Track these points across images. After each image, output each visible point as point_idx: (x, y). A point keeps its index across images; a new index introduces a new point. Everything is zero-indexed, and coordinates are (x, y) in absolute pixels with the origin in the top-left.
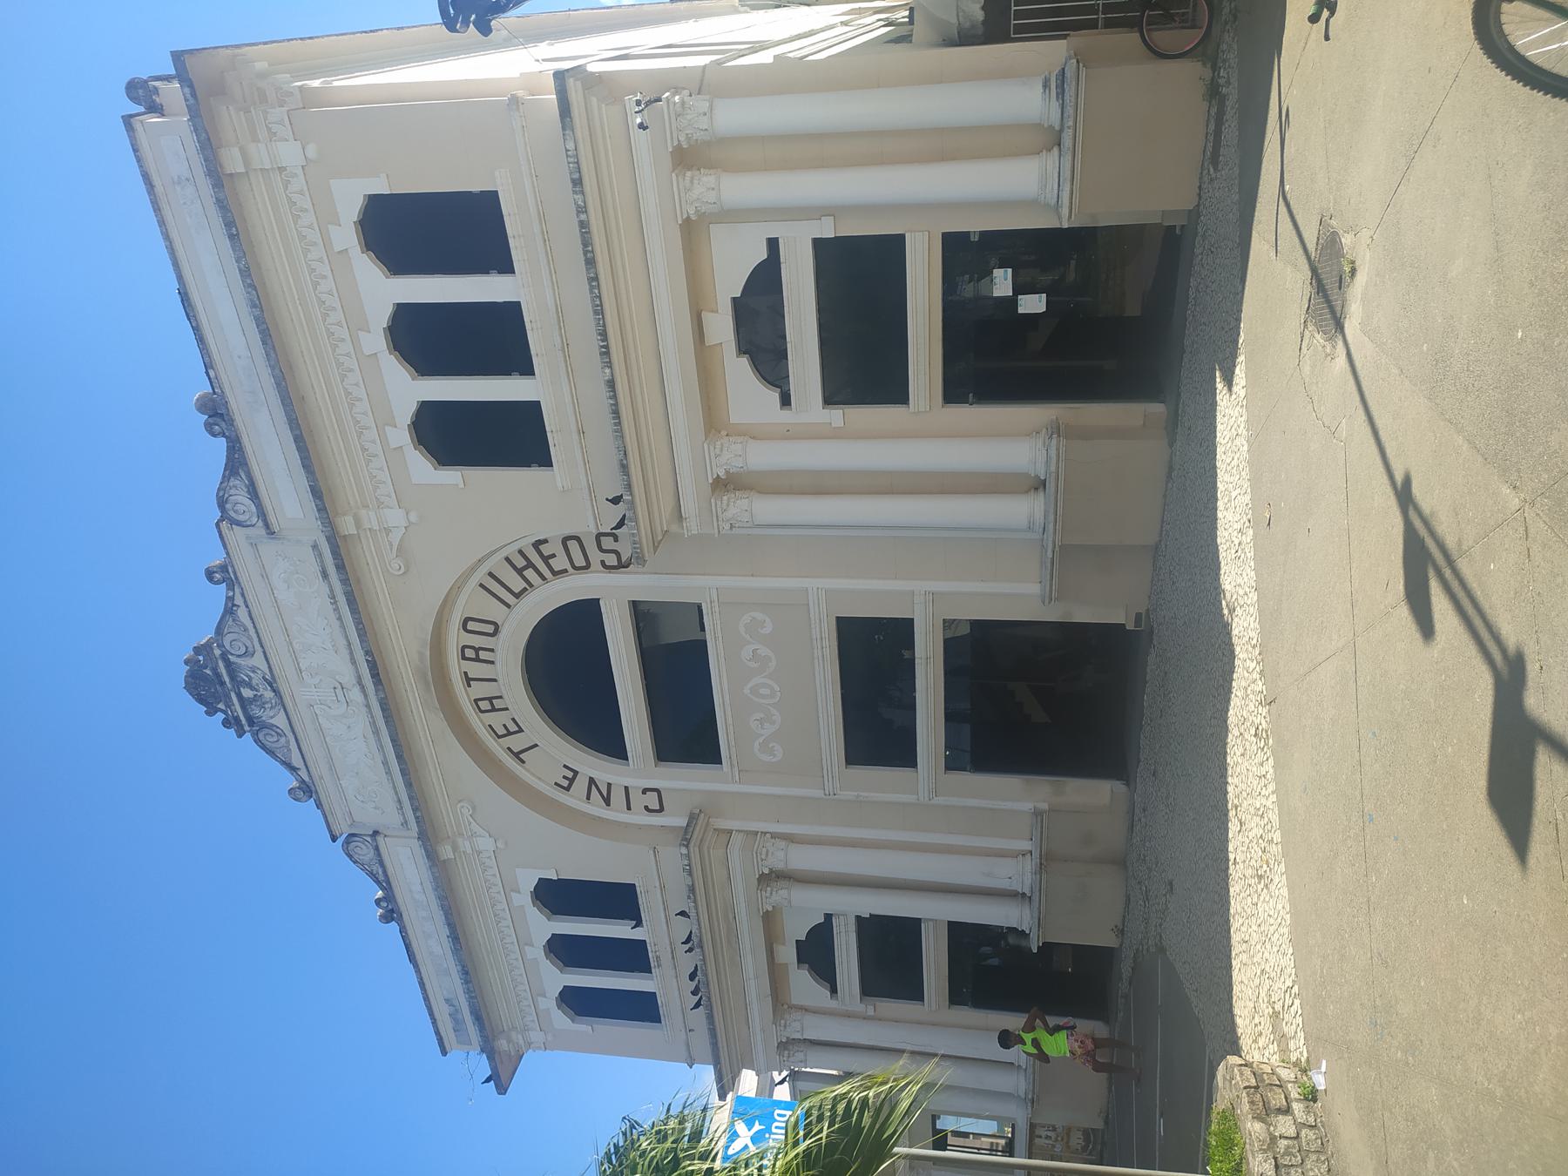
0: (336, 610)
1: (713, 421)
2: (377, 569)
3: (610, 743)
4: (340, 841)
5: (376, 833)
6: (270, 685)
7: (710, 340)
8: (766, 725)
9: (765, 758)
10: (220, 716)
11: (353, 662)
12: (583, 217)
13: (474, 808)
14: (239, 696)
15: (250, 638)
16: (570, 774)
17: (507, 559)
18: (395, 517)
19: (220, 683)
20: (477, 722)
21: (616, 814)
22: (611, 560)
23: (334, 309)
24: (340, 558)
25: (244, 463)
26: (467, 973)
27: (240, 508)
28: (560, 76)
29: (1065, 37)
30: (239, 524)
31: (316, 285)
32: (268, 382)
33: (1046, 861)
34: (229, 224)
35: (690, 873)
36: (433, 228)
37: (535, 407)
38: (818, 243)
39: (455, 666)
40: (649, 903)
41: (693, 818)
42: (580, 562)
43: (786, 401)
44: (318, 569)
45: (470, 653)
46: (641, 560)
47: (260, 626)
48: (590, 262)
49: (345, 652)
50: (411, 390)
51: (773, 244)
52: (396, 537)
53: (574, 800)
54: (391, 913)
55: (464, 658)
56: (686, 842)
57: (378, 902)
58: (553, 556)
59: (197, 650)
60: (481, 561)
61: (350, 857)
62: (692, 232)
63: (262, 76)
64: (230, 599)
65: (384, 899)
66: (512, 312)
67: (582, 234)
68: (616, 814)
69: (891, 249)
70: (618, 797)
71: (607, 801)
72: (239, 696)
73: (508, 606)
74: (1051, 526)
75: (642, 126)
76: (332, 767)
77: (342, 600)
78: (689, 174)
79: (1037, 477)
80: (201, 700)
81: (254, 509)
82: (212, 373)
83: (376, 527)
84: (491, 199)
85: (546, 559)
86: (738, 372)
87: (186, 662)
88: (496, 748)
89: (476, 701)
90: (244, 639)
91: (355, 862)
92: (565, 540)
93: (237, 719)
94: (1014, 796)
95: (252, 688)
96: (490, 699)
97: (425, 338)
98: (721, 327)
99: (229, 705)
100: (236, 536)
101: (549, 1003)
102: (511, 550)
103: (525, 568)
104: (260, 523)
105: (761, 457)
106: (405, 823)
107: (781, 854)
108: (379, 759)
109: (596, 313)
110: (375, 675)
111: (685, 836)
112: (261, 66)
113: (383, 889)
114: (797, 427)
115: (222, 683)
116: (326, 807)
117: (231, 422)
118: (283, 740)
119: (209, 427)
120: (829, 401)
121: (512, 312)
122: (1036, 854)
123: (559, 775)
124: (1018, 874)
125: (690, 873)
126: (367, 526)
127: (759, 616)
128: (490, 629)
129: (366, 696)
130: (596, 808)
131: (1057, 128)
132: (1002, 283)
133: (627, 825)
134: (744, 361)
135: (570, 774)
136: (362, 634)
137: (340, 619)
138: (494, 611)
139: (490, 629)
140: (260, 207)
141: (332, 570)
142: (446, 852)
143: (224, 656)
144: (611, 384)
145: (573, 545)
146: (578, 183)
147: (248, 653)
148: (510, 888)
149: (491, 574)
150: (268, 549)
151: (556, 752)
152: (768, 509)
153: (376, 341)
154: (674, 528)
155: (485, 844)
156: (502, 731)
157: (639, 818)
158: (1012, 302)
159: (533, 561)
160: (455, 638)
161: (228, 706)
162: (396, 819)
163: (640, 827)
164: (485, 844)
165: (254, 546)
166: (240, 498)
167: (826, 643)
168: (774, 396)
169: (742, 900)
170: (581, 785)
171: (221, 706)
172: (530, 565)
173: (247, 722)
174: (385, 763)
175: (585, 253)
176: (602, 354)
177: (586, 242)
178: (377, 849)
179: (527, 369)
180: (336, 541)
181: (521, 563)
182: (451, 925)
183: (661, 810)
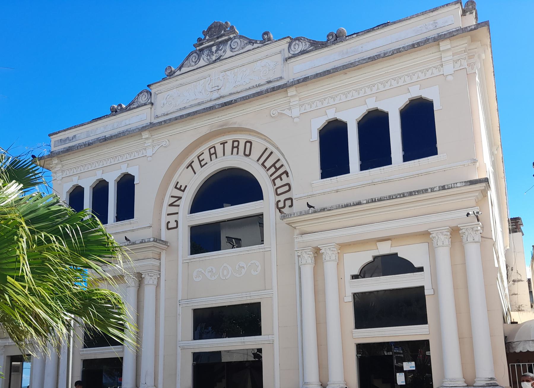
0: (253, 87)
1: (344, 247)
4: (148, 89)
5: (152, 104)
6: (218, 59)
10: (203, 37)
11: (231, 94)
12: (429, 190)
13: (165, 147)
14: (213, 45)
15: (239, 50)
16: (182, 188)
17: (279, 160)
18: (296, 112)
20: (204, 148)
22: (281, 205)
26: (89, 145)
27: (297, 47)
28: (486, 180)
29: (511, 386)
31: (394, 79)
32: (352, 59)
34: (419, 44)
35: (141, 242)
36: (420, 128)
37: (347, 171)
38: (422, 288)
39: (229, 138)
40: (126, 225)
41: (165, 243)
42: (279, 191)
43: (355, 277)
44: (271, 79)
45: (236, 144)
47: (245, 54)
48: (411, 194)
49: (235, 90)
50: (352, 120)
51: (421, 269)
52: (287, 112)
53: (171, 191)
54: (115, 112)
55: (234, 142)
58: (281, 180)
59: (232, 27)
60: (277, 148)
61: (141, 93)
62: (426, 235)
63: (479, 57)
65: (122, 108)
66: (388, 161)
67: (423, 190)
69: (422, 319)
70: (173, 210)
72: (213, 45)
73: (258, 160)
75: (468, 214)
76: (181, 85)
77: (258, 90)
78: (449, 234)
80: (210, 29)
82: (355, 35)
84: (433, 151)
85: (280, 176)
86: (366, 257)
87: (226, 23)
88: (193, 156)
89: (214, 147)
90: (238, 48)
92: (288, 184)
93: (202, 44)
95: (216, 51)
96: (215, 153)
97: (374, 125)
98: (385, 249)
100: (284, 44)
101: (76, 181)
102: (283, 161)
103: (275, 168)
104: (290, 55)
105: (330, 268)
106: (157, 117)
107: (151, 282)
108: (187, 105)
109: (390, 196)
112: (483, 56)
113: (126, 108)
115: (218, 38)
117: (334, 43)
118: (193, 64)
119: (331, 34)
121: (388, 161)
123: (182, 183)
125: (141, 242)
128: (247, 152)
129: (215, 100)
130: (168, 200)
131: (474, 385)
132: (409, 366)
133: (160, 214)
134: (371, 259)
135: (182, 188)
137: (250, 88)
138: (255, 155)
139: (247, 152)
140: (426, 56)
141: (271, 85)
142: (145, 135)
143: (230, 39)
144: (359, 203)
145: (287, 188)
146: (443, 188)
147: (232, 49)
149: (272, 153)
150: (279, 58)
151: (194, 182)
152: (308, 272)
154: (297, 232)
155: (149, 152)
156: (201, 158)
158: (401, 370)
159: (279, 171)
160: (242, 138)
161: (208, 40)
162: (159, 112)
163: (160, 220)
164: (149, 152)
165: (280, 52)
167: (249, 298)
168: (357, 272)
170: (178, 193)
171: (207, 37)
172: (277, 170)
174: (185, 108)
175: (414, 192)
176: (372, 199)
177: (419, 192)
178: (145, 104)
180: (285, 87)
181: (278, 165)
182: (111, 138)
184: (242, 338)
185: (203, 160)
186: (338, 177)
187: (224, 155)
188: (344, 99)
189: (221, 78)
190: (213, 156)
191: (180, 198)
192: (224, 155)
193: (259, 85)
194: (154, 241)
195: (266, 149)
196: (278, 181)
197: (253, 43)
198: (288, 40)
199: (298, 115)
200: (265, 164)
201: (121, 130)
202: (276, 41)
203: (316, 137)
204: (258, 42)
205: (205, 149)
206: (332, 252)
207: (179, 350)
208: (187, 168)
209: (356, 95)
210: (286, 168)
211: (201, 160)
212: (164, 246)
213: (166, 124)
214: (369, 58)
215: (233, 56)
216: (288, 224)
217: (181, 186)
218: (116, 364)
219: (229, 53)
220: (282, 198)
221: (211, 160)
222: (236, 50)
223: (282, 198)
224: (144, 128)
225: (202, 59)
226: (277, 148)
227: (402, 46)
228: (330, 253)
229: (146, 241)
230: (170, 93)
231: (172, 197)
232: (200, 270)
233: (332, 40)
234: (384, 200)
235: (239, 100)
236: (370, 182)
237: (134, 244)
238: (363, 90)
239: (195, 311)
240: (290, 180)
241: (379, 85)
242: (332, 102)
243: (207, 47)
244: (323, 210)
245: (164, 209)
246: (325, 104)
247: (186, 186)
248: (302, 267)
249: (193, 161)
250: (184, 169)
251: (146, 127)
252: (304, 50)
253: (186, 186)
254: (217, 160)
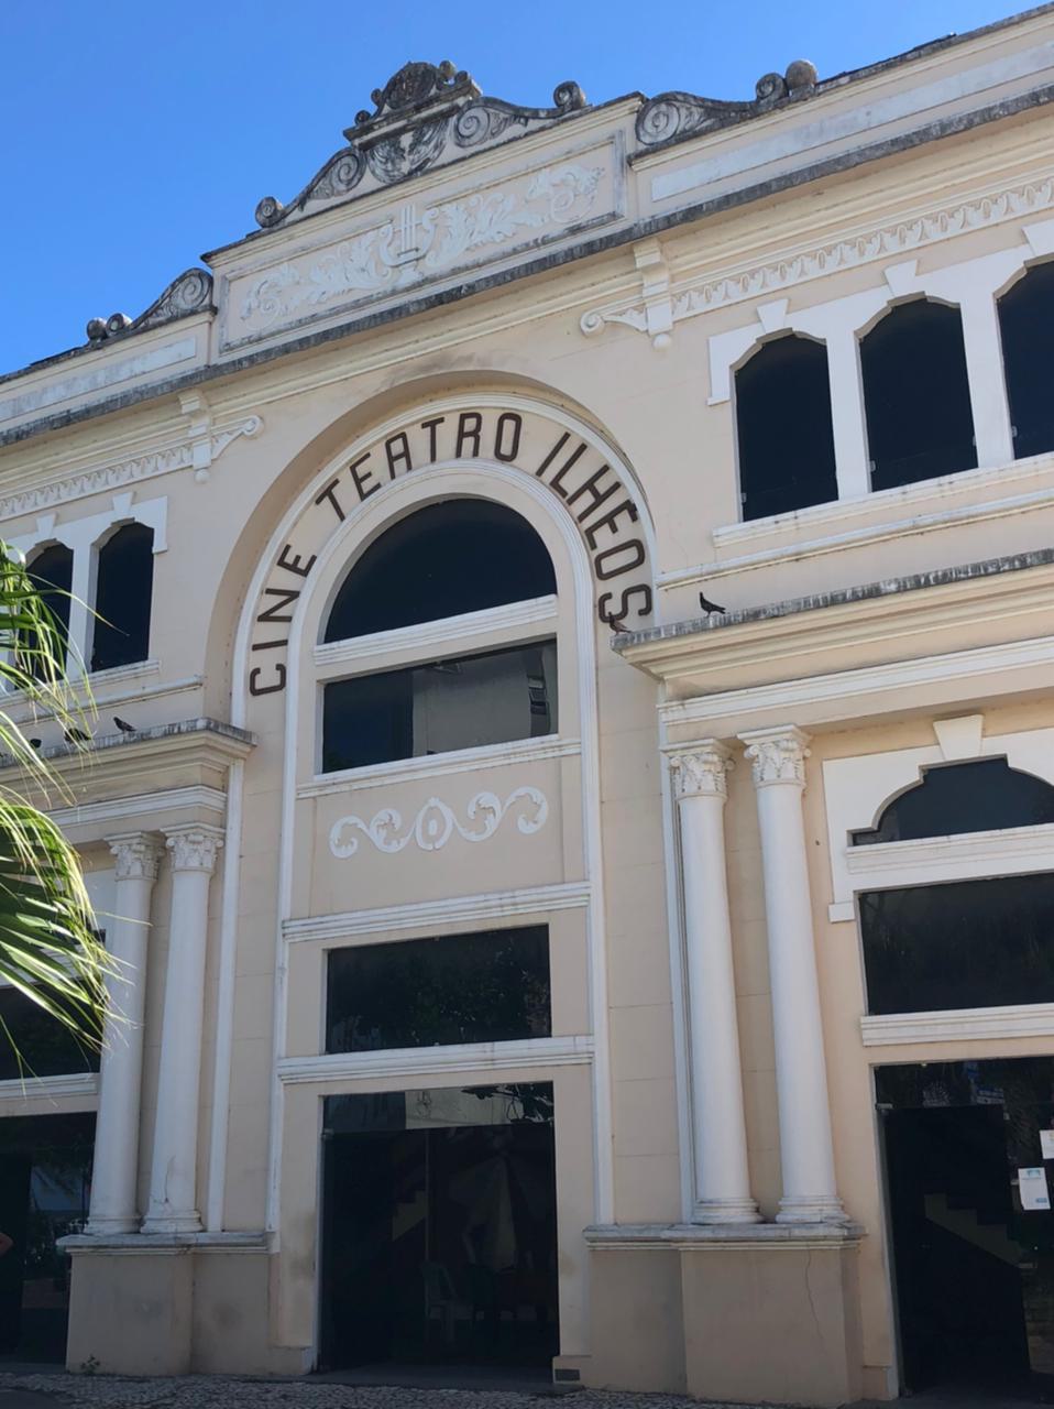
0: (527, 247)
2: (595, 293)
3: (346, 620)
4: (203, 266)
5: (214, 310)
6: (419, 168)
7: (944, 729)
8: (383, 833)
9: (335, 834)
10: (372, 109)
11: (455, 271)
13: (253, 437)
14: (403, 130)
16: (302, 565)
17: (605, 469)
18: (660, 317)
19: (417, 107)
21: (248, 630)
22: (613, 607)
23: (945, 229)
24: (603, 246)
25: (724, 123)
27: (662, 121)
30: (640, 121)
31: (976, 205)
32: (838, 150)
33: (193, 1253)
35: (168, 734)
37: (829, 493)
39: (449, 406)
40: (124, 681)
41: (244, 736)
42: (609, 565)
43: (858, 838)
44: (582, 221)
45: (470, 424)
46: (621, 645)
47: (499, 153)
49: (469, 259)
50: (841, 331)
52: (633, 319)
53: (267, 572)
54: (99, 337)
55: (463, 417)
56: (213, 727)
57: (117, 318)
58: (614, 529)
59: (462, 77)
60: (602, 433)
61: (181, 279)
64: (535, 114)
65: (122, 326)
68: (248, 630)
70: (271, 631)
71: (265, 617)
72: (403, 130)
73: (540, 472)
74: (707, 1233)
79: (779, 1209)
80: (394, 84)
81: (662, 138)
83: (645, 293)
85: (609, 519)
86: (899, 770)
87: (445, 65)
88: (337, 466)
89: (403, 436)
90: (481, 133)
91: (173, 286)
92: (637, 544)
93: (370, 129)
94: (290, 1199)
95: (413, 147)
96: (406, 454)
98: (962, 743)
99: (388, 119)
100: (623, 118)
102: (619, 471)
103: (595, 493)
104: (642, 147)
105: (779, 807)
106: (229, 347)
107: (194, 862)
109: (976, 568)
110: (439, 300)
111: (219, 726)
113: (136, 323)
114: (826, 858)
115: (418, 109)
116: (250, 245)
118: (342, 187)
120: (864, 899)
122: (203, 1238)
123: (301, 550)
124: (172, 1210)
125: (168, 734)
126: (646, 282)
127: (544, 814)
128: (506, 449)
129: (408, 290)
130: (255, 602)
134: (913, 777)
135: (302, 565)
136: (498, 280)
137: (515, 251)
138: (531, 455)
139: (506, 449)
142: (191, 401)
143: (456, 110)
144: (874, 593)
145: (630, 555)
147: (461, 139)
148: (136, 488)
149: (583, 448)
150: (607, 158)
151: (335, 544)
153: (905, 283)
154: (669, 689)
155: (202, 455)
156: (361, 471)
157: (242, 662)
159: (606, 503)
161: (387, 117)
162: (234, 336)
163: (229, 664)
164: (202, 455)
165: (611, 140)
166: (676, 121)
167: (509, 911)
168: (867, 821)
169: (126, 810)
170: (288, 580)
172: (600, 499)
173: (363, 143)
174: (314, 318)
176: (917, 578)
178: (193, 313)
179: (880, 481)
180: (628, 239)
182: (87, 414)
183: (255, 692)
184: (488, 1045)
185: (369, 475)
186: (800, 512)
187: (433, 458)
188: (813, 270)
189: (427, 224)
190: (401, 464)
191: (293, 595)
192: (433, 458)
193: (545, 241)
194: (207, 728)
195: (567, 436)
197: (527, 119)
198: (636, 103)
199: (668, 325)
201: (117, 390)
202: (598, 108)
203: (723, 389)
204: (542, 115)
205: (374, 444)
206: (783, 755)
207: (279, 1090)
208: (318, 501)
209: (853, 258)
210: (631, 491)
211: (360, 476)
212: (239, 746)
213: (255, 368)
214: (894, 142)
215: (463, 159)
216: (639, 665)
217: (298, 558)
218: (77, 1132)
219: (451, 151)
220: (617, 586)
221: (393, 476)
222: (474, 139)
223: (617, 586)
224: (187, 383)
225: (368, 173)
226: (602, 433)
227: (998, 103)
228: (777, 756)
229: (184, 728)
230: (271, 275)
231: (269, 591)
232: (353, 820)
233: (773, 98)
234: (958, 580)
235: (483, 284)
236: (907, 524)
237: (145, 738)
238: (876, 243)
239: (335, 957)
240: (645, 531)
241: (928, 223)
242: (775, 282)
243: (387, 136)
244: (754, 616)
245: (248, 633)
246: (755, 289)
247: (313, 559)
248: (683, 804)
249: (337, 482)
250: (307, 507)
251: (192, 377)
252: (684, 131)
253: (313, 559)
254: (412, 474)
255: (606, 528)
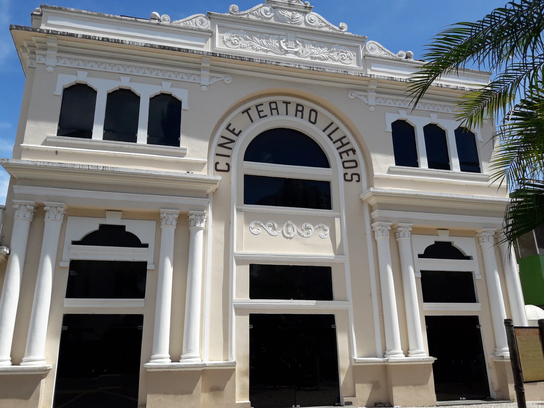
58: (348, 155)
71: (221, 145)
85: (347, 152)
102: (350, 138)
135: (236, 132)
145: (353, 164)
149: (337, 128)
172: (343, 145)
191: (232, 141)
195: (332, 123)
196: (344, 155)
200: (331, 136)
217: (234, 129)
220: (350, 172)
231: (222, 137)
255: (345, 154)
